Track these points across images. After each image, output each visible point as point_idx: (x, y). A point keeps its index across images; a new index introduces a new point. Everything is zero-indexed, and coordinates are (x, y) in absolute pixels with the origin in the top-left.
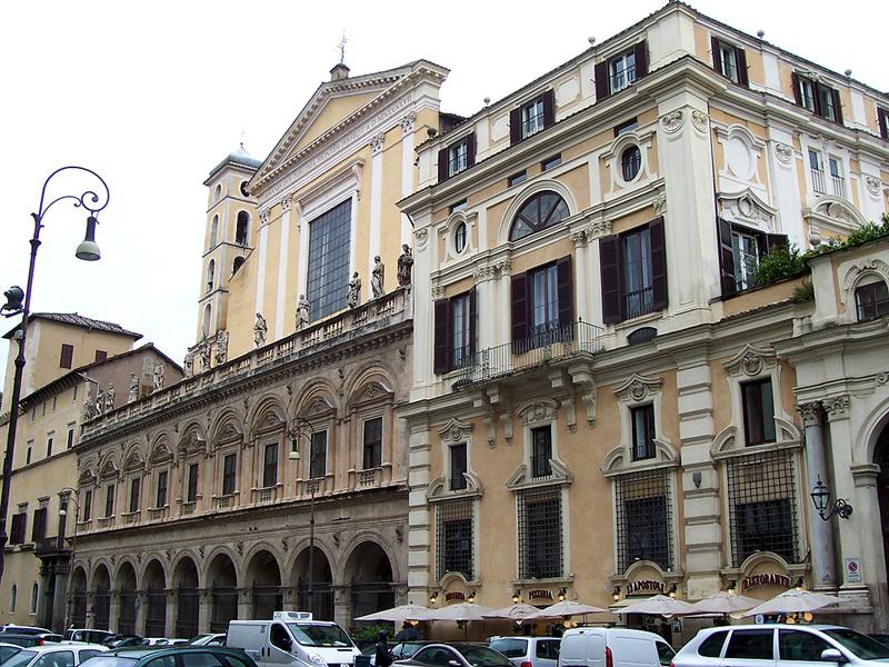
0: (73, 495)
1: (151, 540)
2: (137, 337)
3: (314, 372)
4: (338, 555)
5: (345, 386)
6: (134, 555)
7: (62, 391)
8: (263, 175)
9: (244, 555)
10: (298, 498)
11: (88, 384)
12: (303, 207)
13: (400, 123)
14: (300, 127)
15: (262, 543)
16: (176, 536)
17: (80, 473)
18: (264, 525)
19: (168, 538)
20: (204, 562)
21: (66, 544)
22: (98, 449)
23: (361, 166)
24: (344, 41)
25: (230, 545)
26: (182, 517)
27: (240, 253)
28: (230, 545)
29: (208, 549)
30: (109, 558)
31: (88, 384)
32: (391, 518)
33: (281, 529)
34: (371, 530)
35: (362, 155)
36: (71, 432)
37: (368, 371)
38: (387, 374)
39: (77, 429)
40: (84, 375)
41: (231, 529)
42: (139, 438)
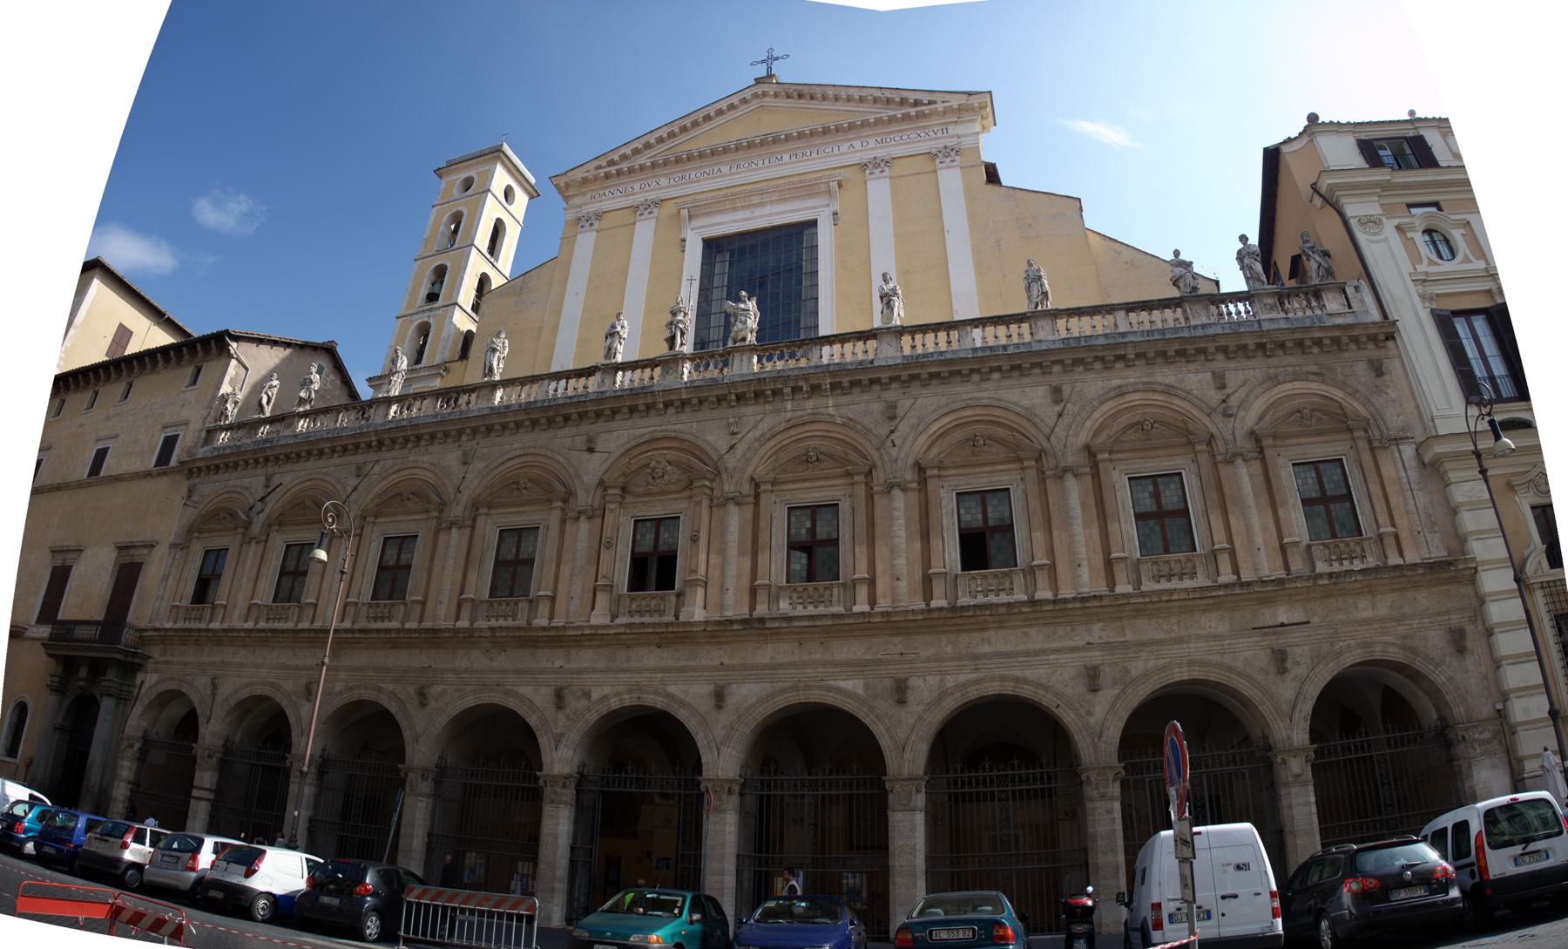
3: (1130, 372)
5: (1233, 401)
8: (600, 167)
9: (915, 707)
12: (690, 217)
13: (934, 151)
14: (695, 124)
15: (1003, 678)
19: (553, 660)
23: (840, 186)
25: (853, 685)
38: (1338, 394)
42: (426, 458)
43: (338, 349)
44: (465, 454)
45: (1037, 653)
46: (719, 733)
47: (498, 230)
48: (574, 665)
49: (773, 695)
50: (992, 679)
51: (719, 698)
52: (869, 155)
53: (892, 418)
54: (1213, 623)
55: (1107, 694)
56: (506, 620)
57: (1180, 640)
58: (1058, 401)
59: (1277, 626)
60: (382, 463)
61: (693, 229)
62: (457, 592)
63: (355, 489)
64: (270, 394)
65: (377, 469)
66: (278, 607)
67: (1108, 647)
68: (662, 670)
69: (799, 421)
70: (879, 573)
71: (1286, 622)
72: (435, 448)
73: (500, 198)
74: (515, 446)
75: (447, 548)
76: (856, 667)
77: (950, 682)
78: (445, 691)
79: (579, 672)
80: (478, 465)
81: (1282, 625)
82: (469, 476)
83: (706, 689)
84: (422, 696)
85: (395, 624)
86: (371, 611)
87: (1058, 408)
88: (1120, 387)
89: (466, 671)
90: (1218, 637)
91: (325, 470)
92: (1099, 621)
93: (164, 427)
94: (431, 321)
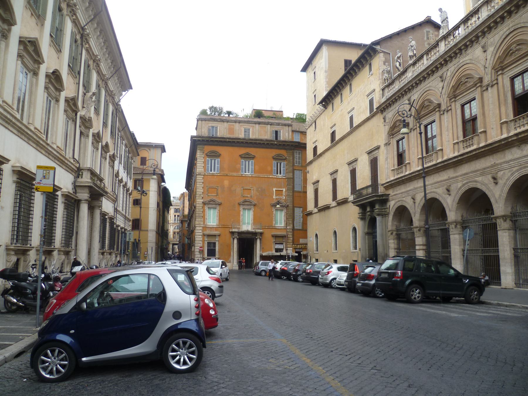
0: (383, 148)
7: (356, 73)
11: (382, 55)
17: (387, 128)
21: (381, 190)
22: (406, 98)
31: (382, 55)
36: (371, 102)
40: (378, 47)
42: (467, 58)
43: (432, 19)
44: (483, 47)
56: (524, 127)
60: (450, 70)
62: (499, 120)
63: (443, 88)
64: (399, 61)
65: (449, 74)
66: (428, 156)
72: (470, 51)
74: (505, 30)
75: (488, 100)
78: (504, 173)
80: (491, 50)
82: (489, 58)
85: (475, 147)
86: (465, 144)
89: (511, 161)
91: (428, 85)
93: (368, 96)
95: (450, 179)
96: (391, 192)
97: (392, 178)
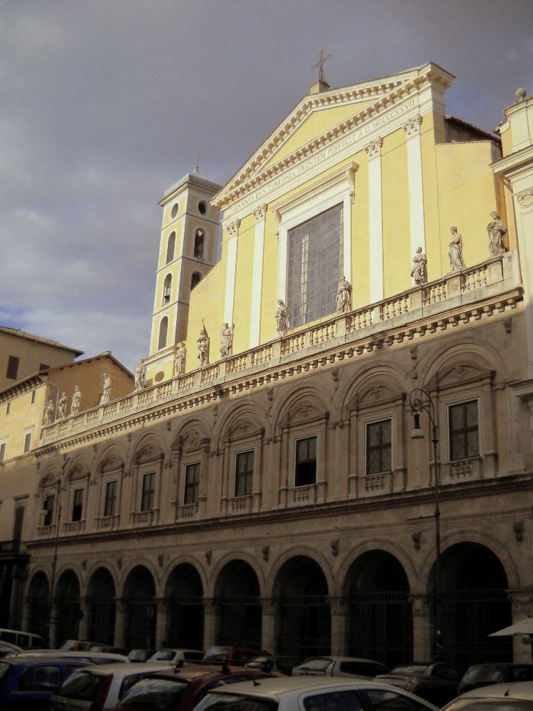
1: (135, 544)
2: (78, 354)
4: (418, 558)
5: (419, 368)
6: (114, 562)
7: (17, 394)
8: (231, 188)
9: (271, 562)
10: (352, 496)
15: (301, 547)
16: (169, 540)
18: (303, 526)
19: (157, 542)
20: (210, 568)
21: (22, 548)
24: (322, 60)
25: (251, 550)
26: (178, 521)
27: (197, 268)
28: (251, 550)
29: (218, 555)
30: (78, 563)
32: (502, 513)
33: (328, 531)
34: (470, 528)
35: (357, 160)
36: (28, 437)
37: (453, 349)
39: (35, 435)
41: (251, 532)
43: (112, 354)
45: (314, 533)
46: (209, 575)
47: (170, 257)
48: (165, 544)
49: (225, 556)
50: (297, 547)
51: (209, 556)
52: (366, 141)
53: (271, 399)
54: (389, 516)
55: (342, 555)
57: (372, 527)
58: (336, 380)
59: (417, 519)
61: (283, 225)
67: (343, 530)
68: (192, 545)
69: (237, 406)
70: (264, 490)
71: (423, 516)
73: (195, 215)
76: (253, 541)
77: (285, 548)
79: (167, 547)
81: (421, 518)
83: (203, 553)
84: (120, 563)
87: (336, 384)
88: (364, 366)
90: (388, 525)
92: (339, 515)
94: (168, 316)
95: (87, 553)
96: (32, 553)
97: (36, 538)
